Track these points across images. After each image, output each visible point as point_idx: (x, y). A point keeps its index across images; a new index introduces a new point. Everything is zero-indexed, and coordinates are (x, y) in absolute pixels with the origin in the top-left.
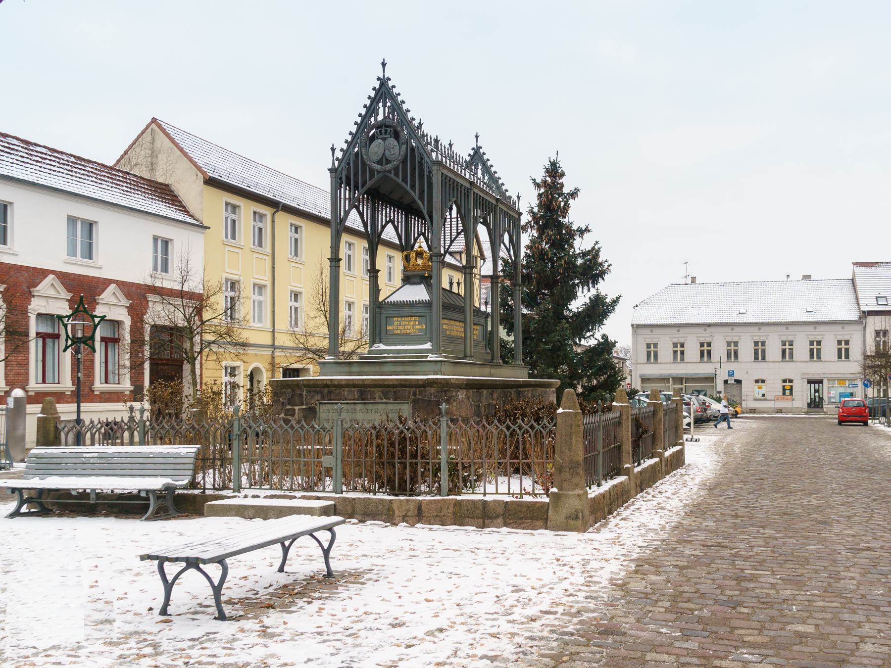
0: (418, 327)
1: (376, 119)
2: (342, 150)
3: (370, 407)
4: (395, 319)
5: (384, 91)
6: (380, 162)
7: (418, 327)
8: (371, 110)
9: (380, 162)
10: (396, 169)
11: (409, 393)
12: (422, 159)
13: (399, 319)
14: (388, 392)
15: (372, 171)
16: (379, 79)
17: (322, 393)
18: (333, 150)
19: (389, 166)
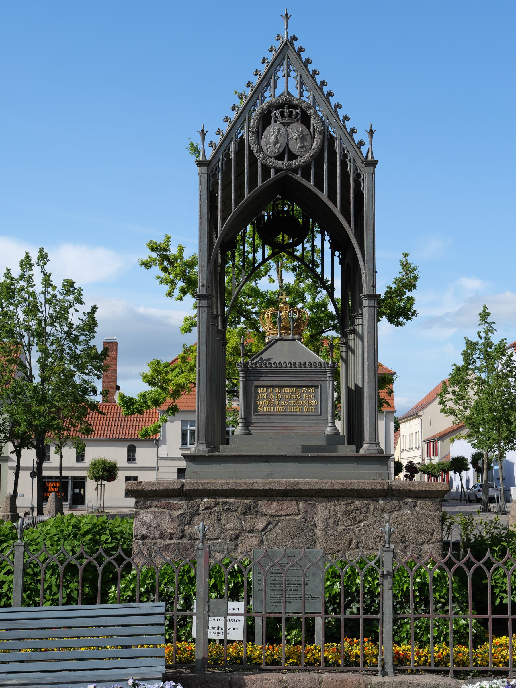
6: (280, 157)
8: (267, 80)
9: (280, 157)
10: (305, 169)
12: (345, 156)
15: (266, 169)
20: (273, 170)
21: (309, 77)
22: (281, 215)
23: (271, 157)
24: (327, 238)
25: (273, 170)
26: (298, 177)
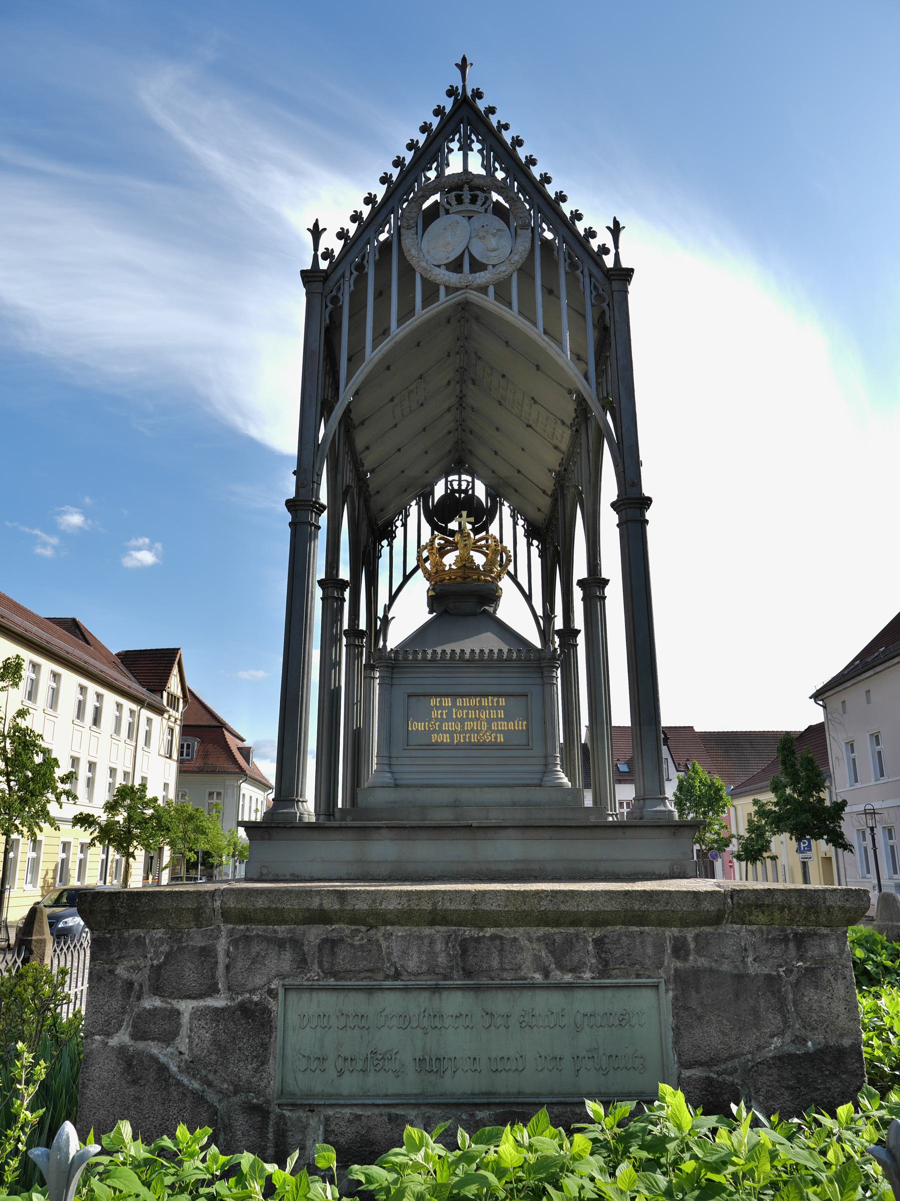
0: (503, 726)
1: (440, 174)
2: (342, 234)
3: (500, 1002)
4: (433, 702)
5: (465, 116)
6: (456, 266)
7: (503, 726)
11: (660, 948)
13: (447, 702)
14: (569, 943)
15: (431, 292)
16: (451, 92)
17: (296, 943)
18: (316, 232)
19: (481, 278)
20: (442, 290)
21: (500, 150)
22: (457, 495)
23: (439, 266)
24: (521, 522)
25: (442, 290)
26: (489, 301)
